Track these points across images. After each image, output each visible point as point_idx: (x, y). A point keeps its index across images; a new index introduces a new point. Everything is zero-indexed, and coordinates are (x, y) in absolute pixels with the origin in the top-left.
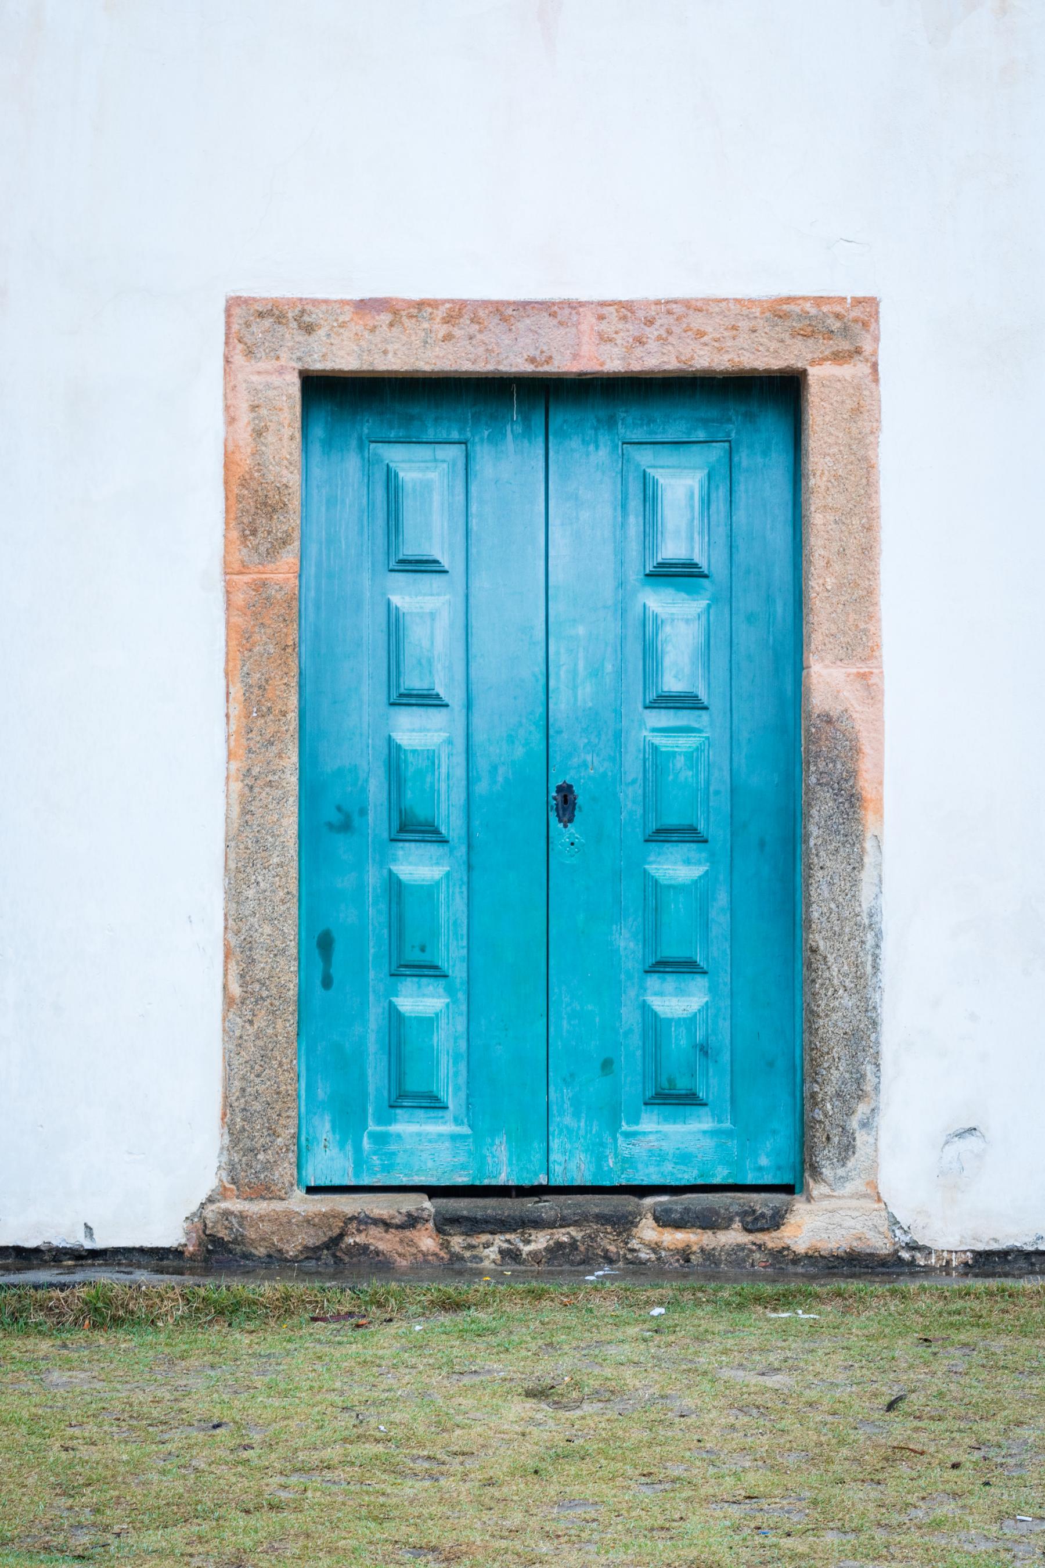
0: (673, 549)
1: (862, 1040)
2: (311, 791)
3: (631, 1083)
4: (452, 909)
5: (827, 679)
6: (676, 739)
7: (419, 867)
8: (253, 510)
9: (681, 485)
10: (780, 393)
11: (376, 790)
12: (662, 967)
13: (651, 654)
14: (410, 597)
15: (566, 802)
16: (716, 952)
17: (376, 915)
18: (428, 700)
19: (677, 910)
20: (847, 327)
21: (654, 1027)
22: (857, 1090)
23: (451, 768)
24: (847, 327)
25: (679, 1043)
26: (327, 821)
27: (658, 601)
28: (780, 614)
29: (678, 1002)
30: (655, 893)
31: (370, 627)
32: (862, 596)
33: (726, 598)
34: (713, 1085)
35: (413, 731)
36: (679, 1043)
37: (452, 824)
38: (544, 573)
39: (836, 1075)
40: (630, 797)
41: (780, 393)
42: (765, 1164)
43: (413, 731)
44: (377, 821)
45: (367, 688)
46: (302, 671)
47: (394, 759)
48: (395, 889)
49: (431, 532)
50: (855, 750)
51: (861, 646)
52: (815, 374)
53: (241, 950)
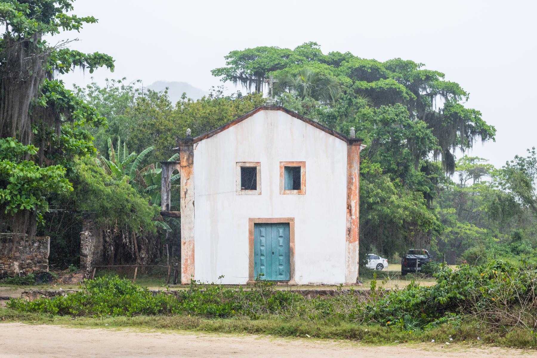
0: (281, 235)
1: (294, 270)
2: (255, 253)
3: (278, 273)
4: (265, 261)
5: (291, 244)
6: (281, 249)
7: (262, 258)
8: (251, 233)
9: (281, 231)
10: (288, 224)
11: (259, 252)
12: (280, 265)
13: (279, 242)
14: (262, 238)
15: (273, 253)
16: (284, 264)
17: (259, 261)
18: (263, 246)
19: (281, 261)
20: (293, 220)
21: (279, 269)
22: (294, 273)
23: (265, 251)
24: (293, 220)
25: (281, 270)
26: (256, 254)
27: (280, 239)
28: (288, 240)
29: (281, 267)
30: (279, 260)
31: (259, 241)
32: (294, 239)
33: (285, 238)
34: (284, 273)
35: (262, 248)
36: (281, 270)
37: (265, 254)
38: (271, 237)
39: (292, 272)
40: (278, 253)
41: (288, 224)
42: (287, 279)
43: (262, 248)
44: (259, 254)
45: (259, 245)
46: (254, 244)
47: (261, 250)
48: (261, 259)
49: (263, 234)
50: (293, 249)
51: (294, 242)
52: (290, 223)
53: (250, 264)
